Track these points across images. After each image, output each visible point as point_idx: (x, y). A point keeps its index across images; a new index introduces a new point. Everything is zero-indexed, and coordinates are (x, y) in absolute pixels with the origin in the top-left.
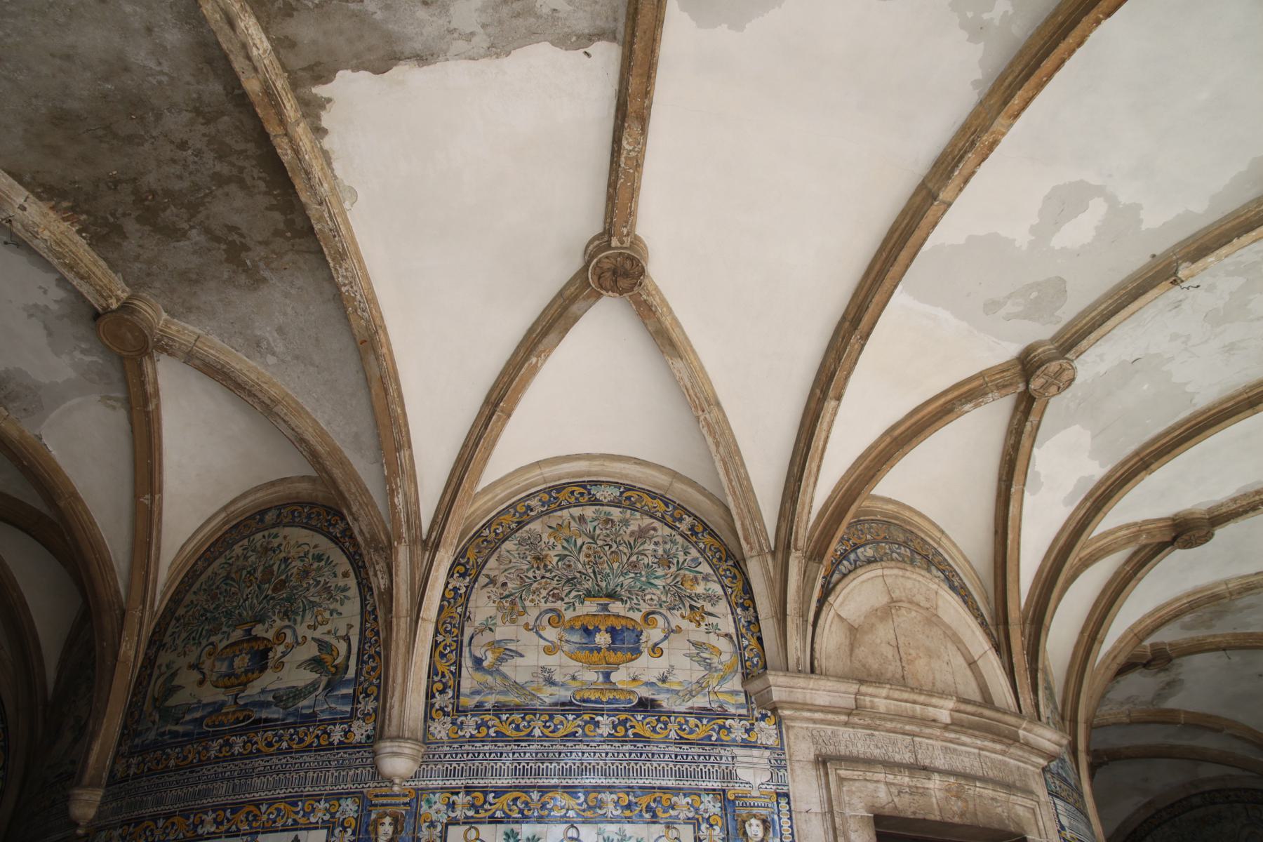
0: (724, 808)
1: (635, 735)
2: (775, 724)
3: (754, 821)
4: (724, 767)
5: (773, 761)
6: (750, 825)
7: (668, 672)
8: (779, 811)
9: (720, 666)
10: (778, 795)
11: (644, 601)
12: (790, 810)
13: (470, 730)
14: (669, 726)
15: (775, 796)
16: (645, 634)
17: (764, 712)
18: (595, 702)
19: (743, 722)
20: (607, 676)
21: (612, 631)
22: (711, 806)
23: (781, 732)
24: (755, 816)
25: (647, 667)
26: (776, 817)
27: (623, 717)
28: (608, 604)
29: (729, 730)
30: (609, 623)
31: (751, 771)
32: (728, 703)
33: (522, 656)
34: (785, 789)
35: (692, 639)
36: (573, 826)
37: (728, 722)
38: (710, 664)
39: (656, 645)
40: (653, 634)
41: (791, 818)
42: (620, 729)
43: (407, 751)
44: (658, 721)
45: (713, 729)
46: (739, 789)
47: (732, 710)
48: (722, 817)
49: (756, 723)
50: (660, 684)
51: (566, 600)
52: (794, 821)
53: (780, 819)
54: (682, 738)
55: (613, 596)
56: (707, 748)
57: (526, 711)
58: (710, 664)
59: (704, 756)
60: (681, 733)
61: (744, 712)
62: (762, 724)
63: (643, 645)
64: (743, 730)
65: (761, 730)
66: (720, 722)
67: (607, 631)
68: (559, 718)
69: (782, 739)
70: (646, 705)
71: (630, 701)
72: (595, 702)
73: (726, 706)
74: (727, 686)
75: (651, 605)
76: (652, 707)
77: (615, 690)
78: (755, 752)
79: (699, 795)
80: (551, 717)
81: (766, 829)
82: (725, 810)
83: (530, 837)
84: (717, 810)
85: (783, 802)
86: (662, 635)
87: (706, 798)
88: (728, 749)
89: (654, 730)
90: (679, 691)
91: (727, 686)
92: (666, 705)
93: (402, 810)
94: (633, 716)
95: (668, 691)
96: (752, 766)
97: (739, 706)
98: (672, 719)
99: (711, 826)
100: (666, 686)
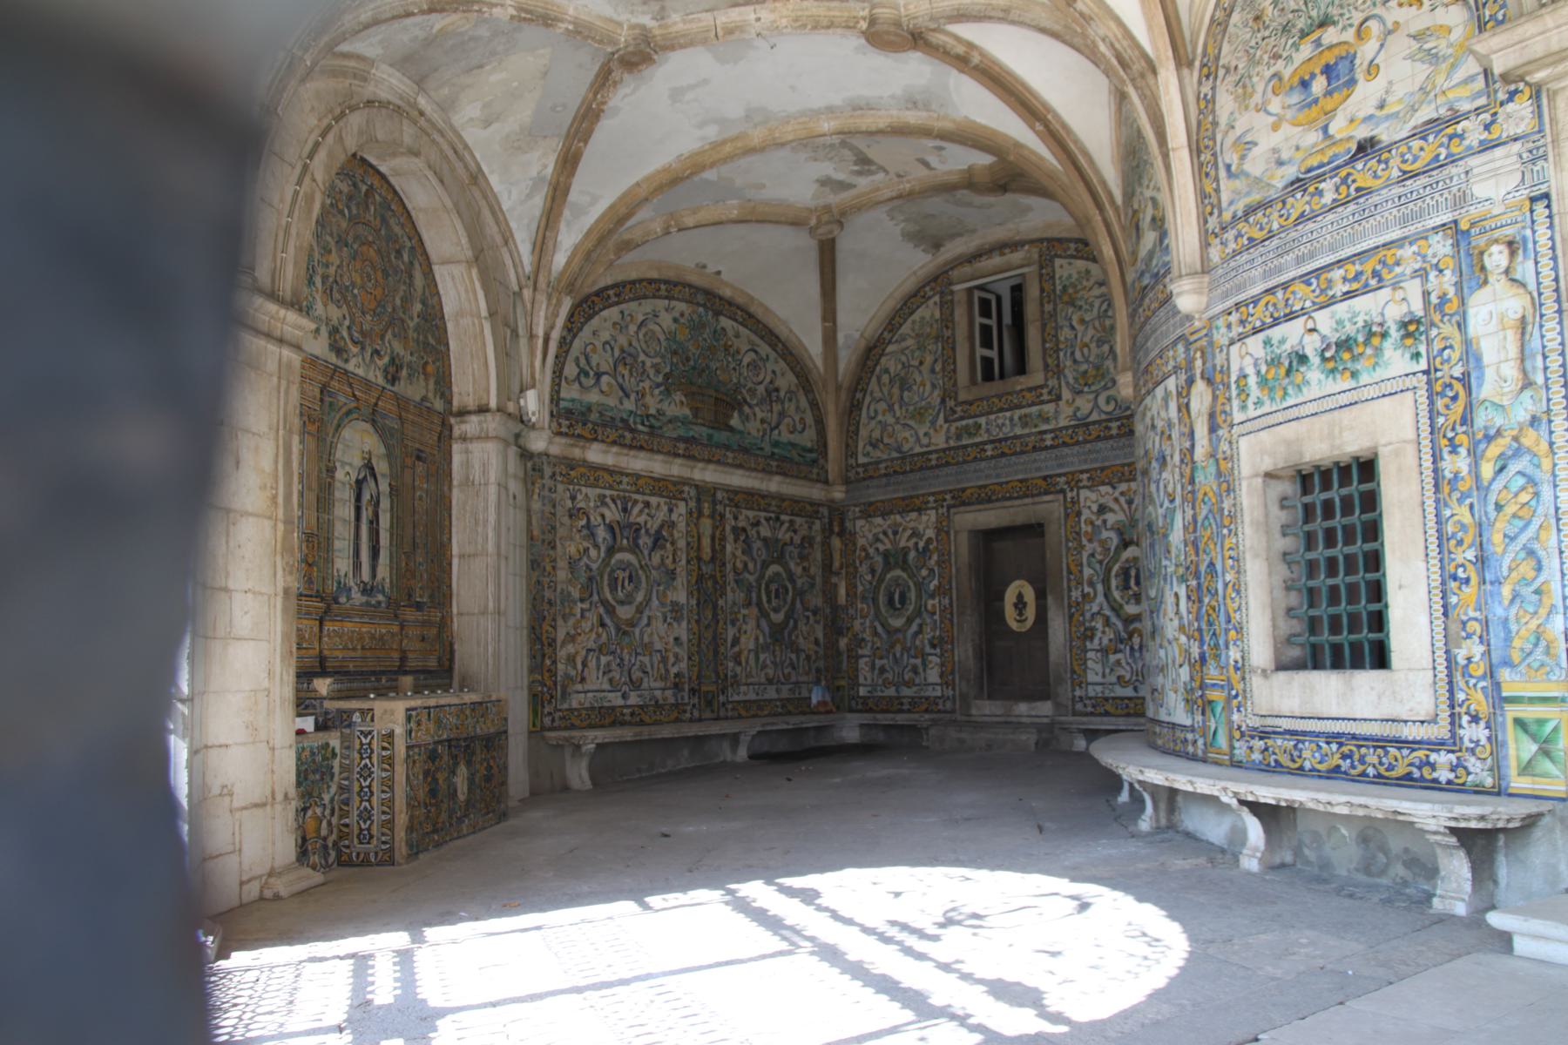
0: (1456, 245)
1: (1358, 190)
2: (1531, 97)
3: (1495, 249)
4: (1455, 190)
5: (1525, 155)
6: (1490, 255)
7: (1387, 92)
8: (1533, 222)
9: (1450, 51)
10: (1533, 200)
11: (1356, 8)
12: (1550, 217)
13: (1232, 246)
14: (1391, 163)
15: (1527, 203)
16: (1358, 55)
17: (1513, 87)
18: (1319, 167)
19: (1482, 116)
20: (1325, 129)
21: (1328, 70)
22: (1441, 247)
23: (1539, 107)
24: (1496, 241)
25: (1365, 95)
26: (1528, 232)
27: (1343, 173)
28: (1320, 38)
29: (1461, 137)
30: (1323, 62)
31: (1492, 181)
32: (1459, 99)
33: (1256, 144)
34: (1543, 189)
35: (1413, 31)
36: (1310, 317)
37: (1459, 128)
38: (1436, 55)
39: (1372, 61)
40: (1367, 50)
41: (1551, 227)
42: (1343, 189)
43: (1186, 288)
44: (1379, 162)
45: (1441, 145)
46: (1474, 212)
47: (1466, 107)
48: (1453, 257)
49: (1500, 110)
50: (1379, 113)
51: (1285, 55)
52: (1557, 228)
53: (1534, 232)
54: (1405, 172)
55: (1325, 23)
56: (1434, 173)
57: (1264, 205)
58: (1436, 55)
59: (1444, 181)
60: (1406, 167)
61: (1482, 101)
62: (1510, 107)
63: (1358, 70)
64: (1482, 127)
65: (1509, 116)
66: (1450, 131)
67: (1322, 73)
68: (1290, 200)
69: (1540, 116)
70: (1366, 148)
71: (1349, 151)
72: (1319, 167)
73: (1457, 106)
74: (1460, 75)
75: (1363, 11)
76: (1372, 146)
77: (1334, 143)
78: (1499, 152)
79: (1426, 238)
80: (1284, 202)
81: (1513, 254)
82: (1458, 246)
83: (1335, 326)
84: (1448, 250)
85: (1540, 208)
86: (1377, 45)
87: (1435, 239)
88: (1460, 163)
89: (1376, 177)
90: (1398, 113)
91: (1460, 75)
92: (1385, 138)
93: (1203, 343)
94: (1353, 167)
95: (1388, 117)
96: (1495, 174)
97: (1478, 95)
98: (1393, 152)
99: (1441, 271)
100: (1385, 112)
